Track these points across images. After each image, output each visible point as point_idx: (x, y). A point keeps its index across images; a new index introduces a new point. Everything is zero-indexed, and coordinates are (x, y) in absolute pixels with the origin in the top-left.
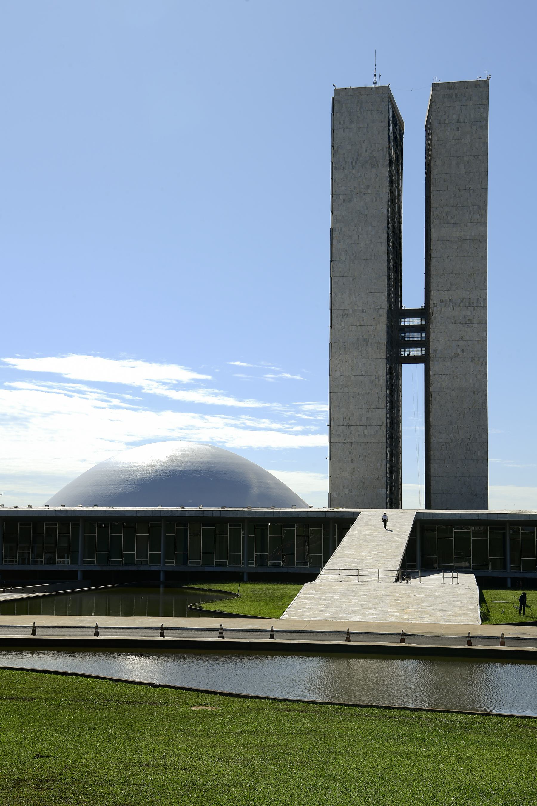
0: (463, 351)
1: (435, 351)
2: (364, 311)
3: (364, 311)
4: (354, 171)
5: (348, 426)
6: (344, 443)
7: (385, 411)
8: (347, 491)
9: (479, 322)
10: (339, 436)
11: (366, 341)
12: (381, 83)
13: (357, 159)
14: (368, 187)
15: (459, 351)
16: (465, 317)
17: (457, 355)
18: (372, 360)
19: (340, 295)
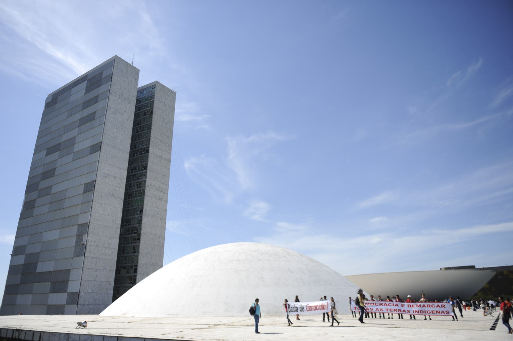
0: (157, 214)
1: (146, 210)
2: (115, 177)
3: (115, 177)
4: (120, 100)
5: (97, 246)
6: (93, 258)
7: (118, 240)
8: (90, 291)
9: (165, 201)
10: (90, 252)
11: (113, 195)
12: (134, 65)
13: (122, 95)
14: (125, 112)
15: (155, 214)
16: (159, 196)
17: (154, 216)
18: (115, 207)
19: (103, 164)
